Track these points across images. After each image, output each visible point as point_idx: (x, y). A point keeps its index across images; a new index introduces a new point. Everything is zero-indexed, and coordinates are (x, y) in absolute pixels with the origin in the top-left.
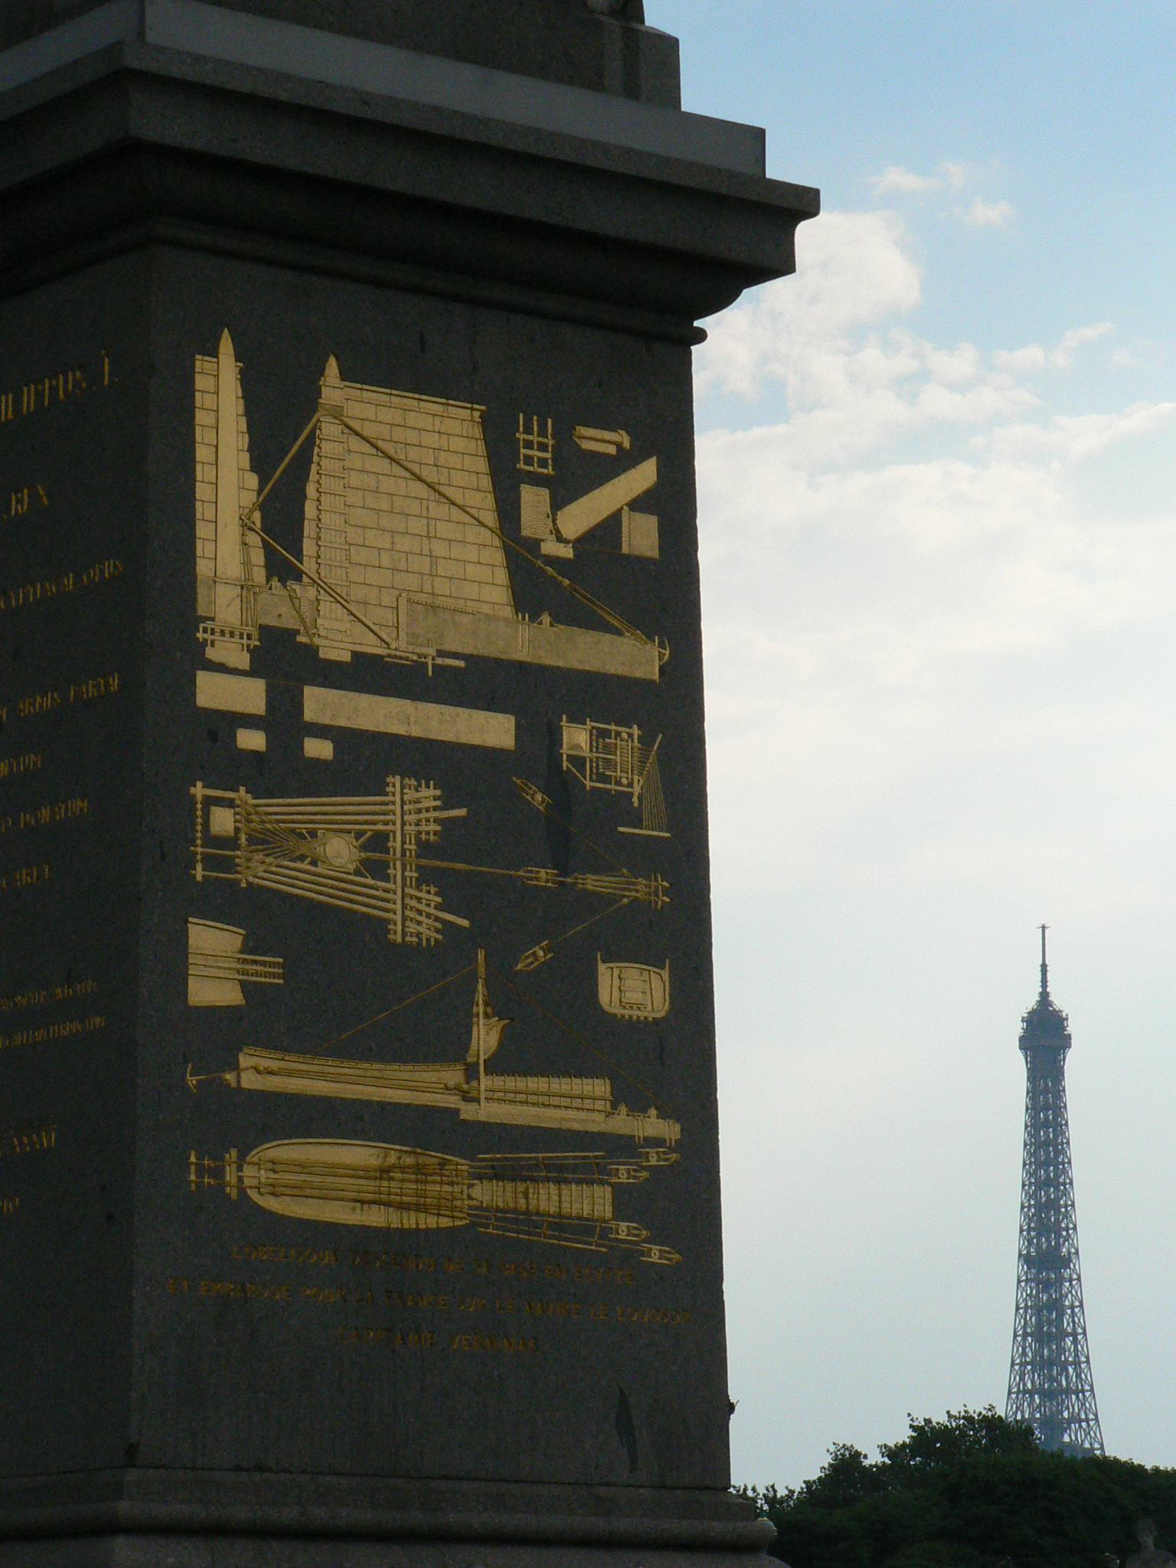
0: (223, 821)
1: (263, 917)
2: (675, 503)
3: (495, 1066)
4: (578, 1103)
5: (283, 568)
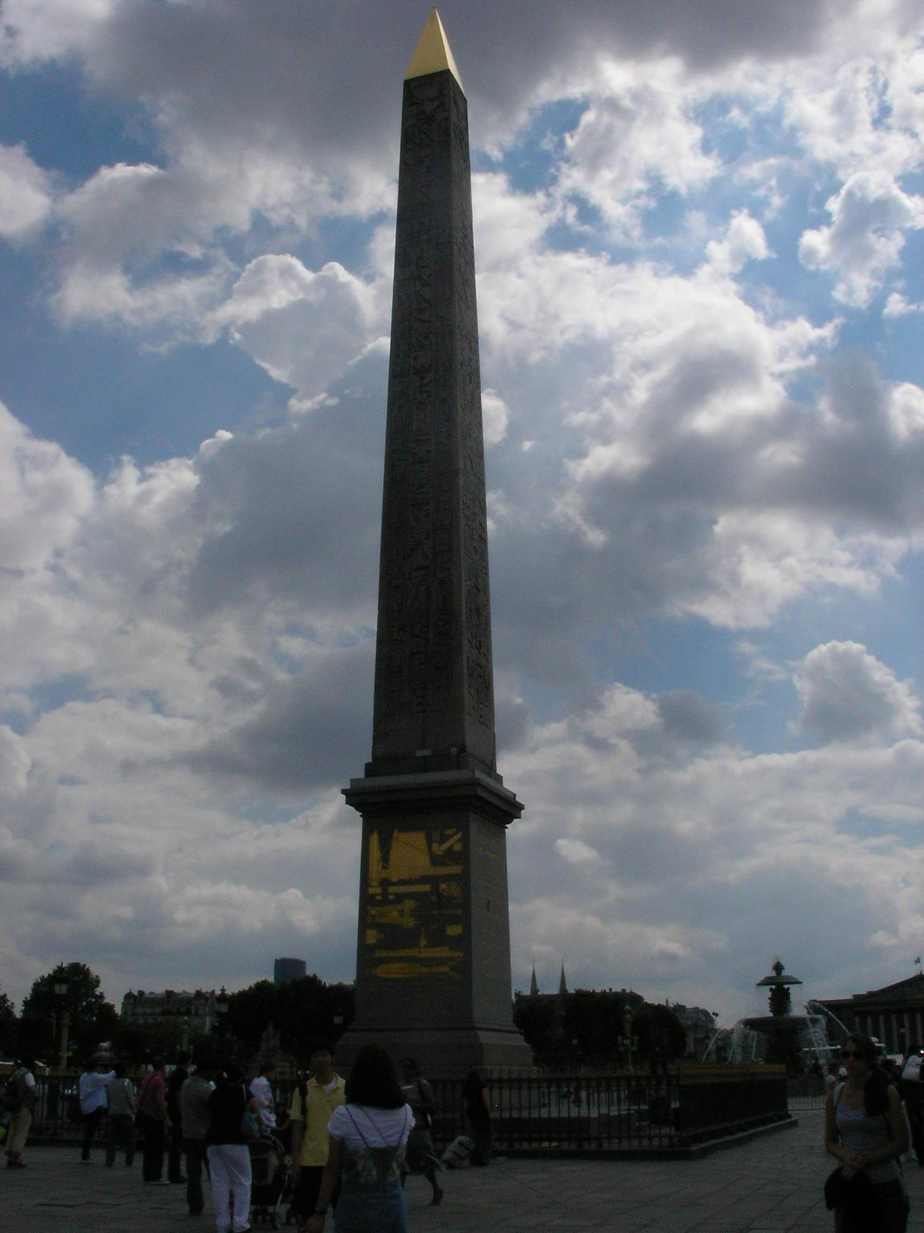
0: (373, 912)
1: (381, 928)
2: (465, 841)
3: (425, 947)
4: (443, 952)
5: (384, 868)
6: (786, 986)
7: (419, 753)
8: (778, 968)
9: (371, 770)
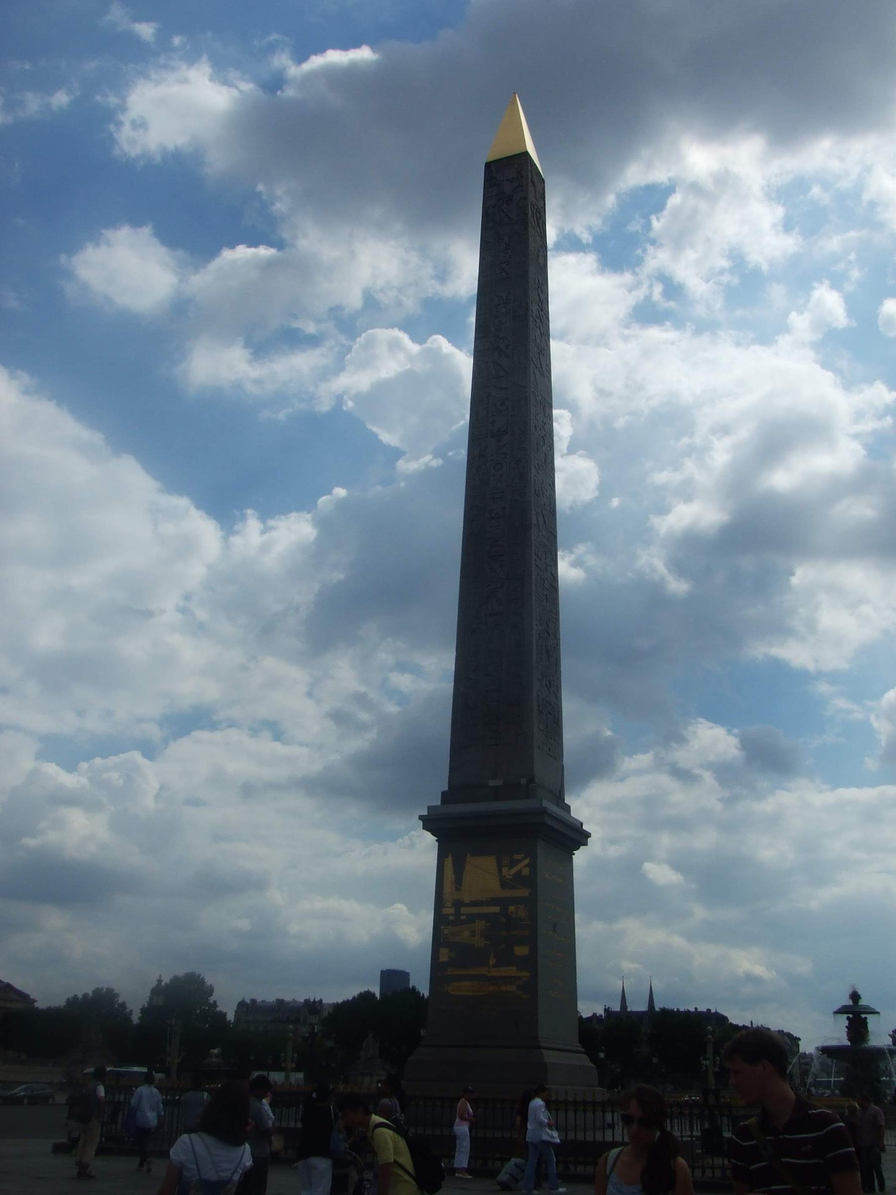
0: (446, 931)
2: (533, 866)
3: (494, 966)
4: (511, 971)
5: (458, 890)
6: (863, 1016)
7: (492, 783)
8: (855, 997)
9: (446, 798)
